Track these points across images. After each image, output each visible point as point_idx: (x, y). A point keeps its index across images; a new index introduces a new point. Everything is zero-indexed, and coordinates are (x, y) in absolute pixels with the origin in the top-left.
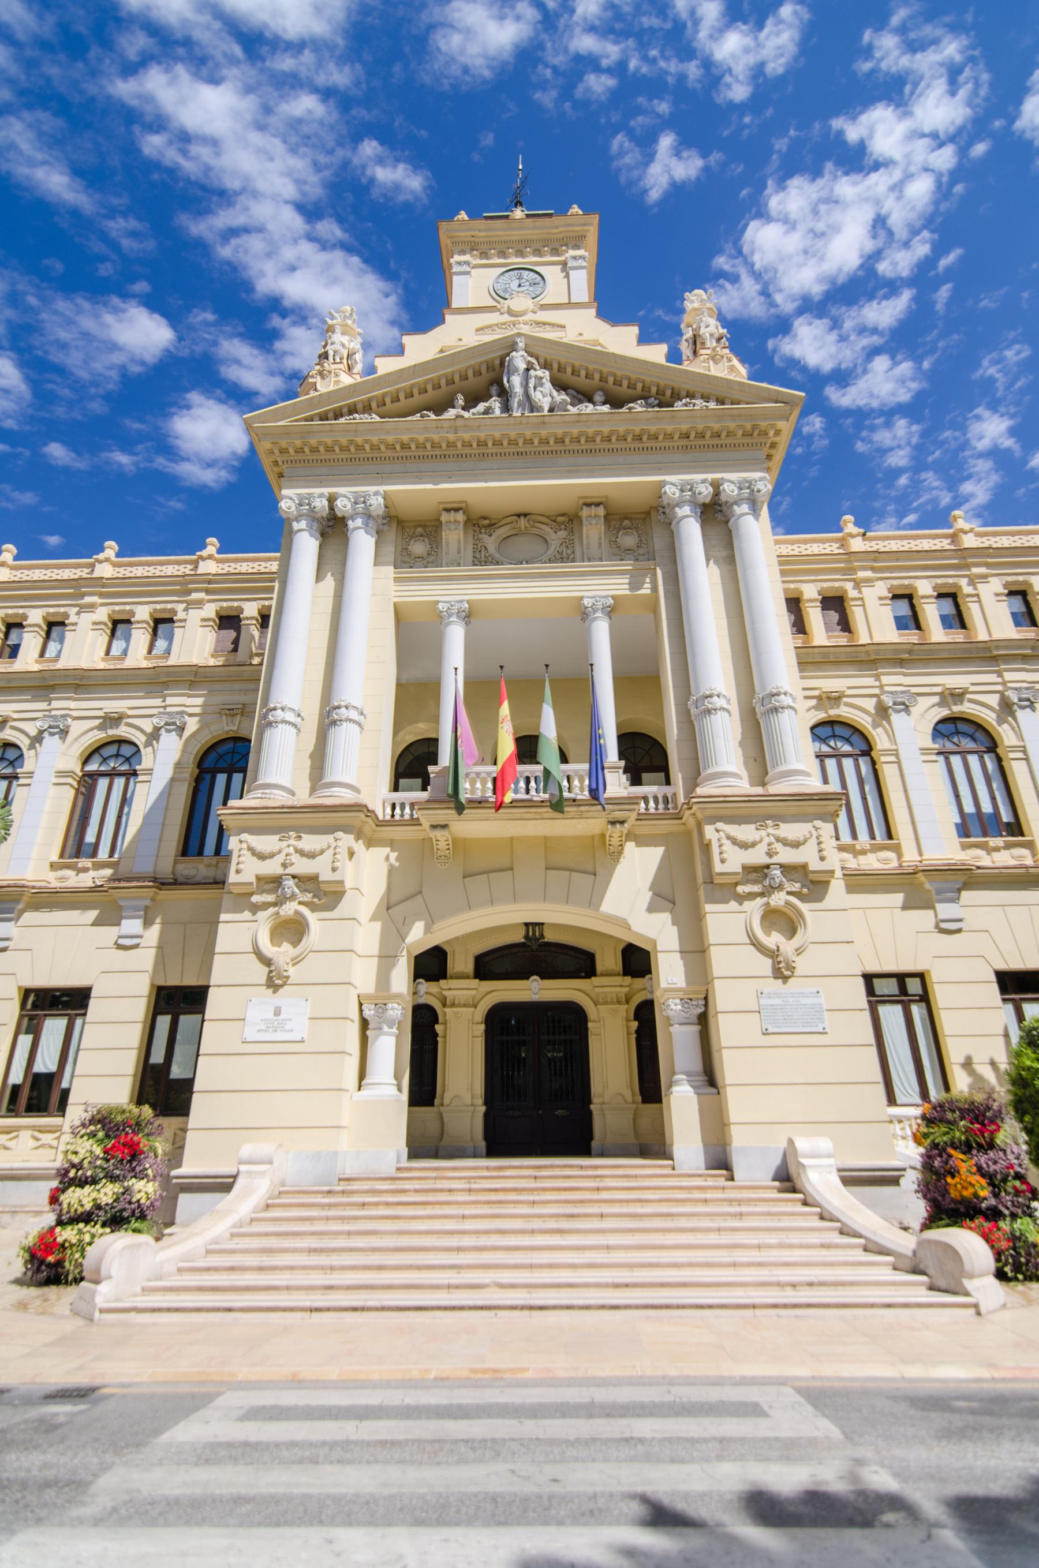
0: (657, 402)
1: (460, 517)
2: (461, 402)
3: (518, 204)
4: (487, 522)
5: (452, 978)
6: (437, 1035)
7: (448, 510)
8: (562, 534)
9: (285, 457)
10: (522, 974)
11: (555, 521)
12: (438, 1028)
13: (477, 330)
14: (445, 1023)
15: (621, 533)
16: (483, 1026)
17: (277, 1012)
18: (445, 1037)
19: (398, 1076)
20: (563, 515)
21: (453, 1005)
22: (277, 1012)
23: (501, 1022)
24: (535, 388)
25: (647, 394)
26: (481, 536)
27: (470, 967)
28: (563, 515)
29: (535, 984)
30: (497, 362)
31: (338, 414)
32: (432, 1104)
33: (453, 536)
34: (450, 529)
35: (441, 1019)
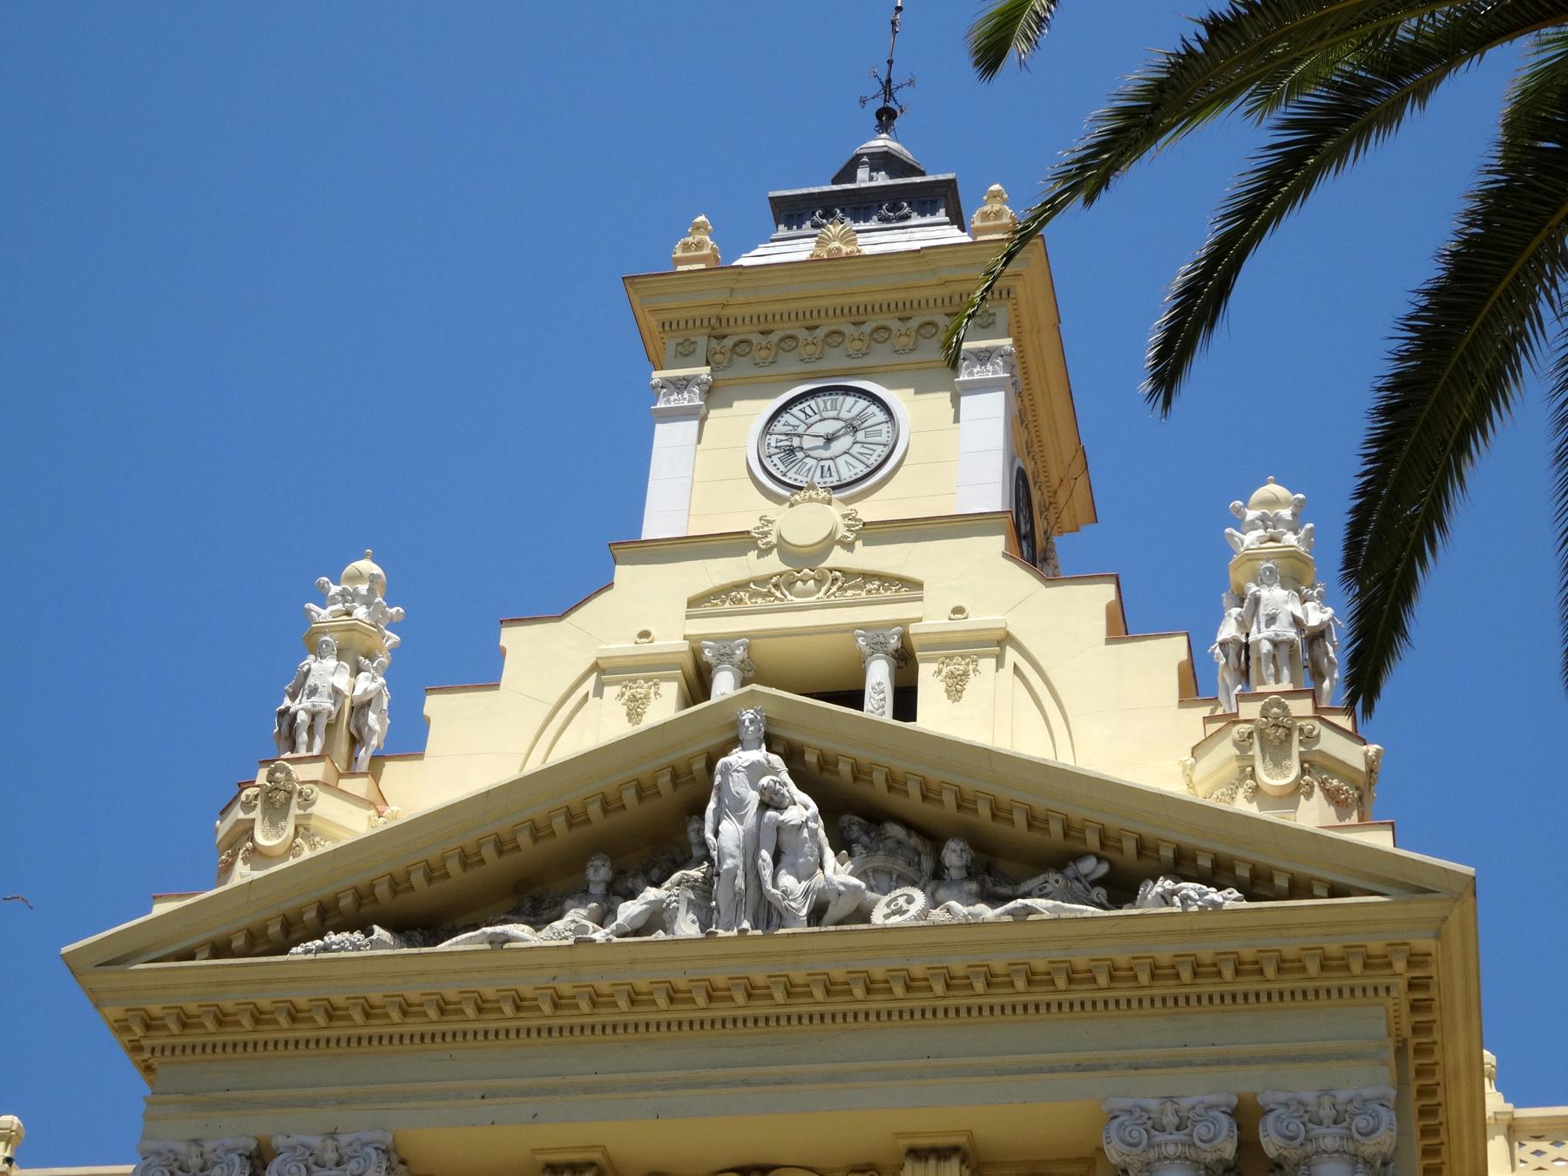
0: (1104, 869)
2: (598, 873)
3: (886, 118)
9: (158, 1039)
13: (693, 603)
24: (777, 858)
25: (1079, 847)
30: (700, 765)
31: (293, 931)
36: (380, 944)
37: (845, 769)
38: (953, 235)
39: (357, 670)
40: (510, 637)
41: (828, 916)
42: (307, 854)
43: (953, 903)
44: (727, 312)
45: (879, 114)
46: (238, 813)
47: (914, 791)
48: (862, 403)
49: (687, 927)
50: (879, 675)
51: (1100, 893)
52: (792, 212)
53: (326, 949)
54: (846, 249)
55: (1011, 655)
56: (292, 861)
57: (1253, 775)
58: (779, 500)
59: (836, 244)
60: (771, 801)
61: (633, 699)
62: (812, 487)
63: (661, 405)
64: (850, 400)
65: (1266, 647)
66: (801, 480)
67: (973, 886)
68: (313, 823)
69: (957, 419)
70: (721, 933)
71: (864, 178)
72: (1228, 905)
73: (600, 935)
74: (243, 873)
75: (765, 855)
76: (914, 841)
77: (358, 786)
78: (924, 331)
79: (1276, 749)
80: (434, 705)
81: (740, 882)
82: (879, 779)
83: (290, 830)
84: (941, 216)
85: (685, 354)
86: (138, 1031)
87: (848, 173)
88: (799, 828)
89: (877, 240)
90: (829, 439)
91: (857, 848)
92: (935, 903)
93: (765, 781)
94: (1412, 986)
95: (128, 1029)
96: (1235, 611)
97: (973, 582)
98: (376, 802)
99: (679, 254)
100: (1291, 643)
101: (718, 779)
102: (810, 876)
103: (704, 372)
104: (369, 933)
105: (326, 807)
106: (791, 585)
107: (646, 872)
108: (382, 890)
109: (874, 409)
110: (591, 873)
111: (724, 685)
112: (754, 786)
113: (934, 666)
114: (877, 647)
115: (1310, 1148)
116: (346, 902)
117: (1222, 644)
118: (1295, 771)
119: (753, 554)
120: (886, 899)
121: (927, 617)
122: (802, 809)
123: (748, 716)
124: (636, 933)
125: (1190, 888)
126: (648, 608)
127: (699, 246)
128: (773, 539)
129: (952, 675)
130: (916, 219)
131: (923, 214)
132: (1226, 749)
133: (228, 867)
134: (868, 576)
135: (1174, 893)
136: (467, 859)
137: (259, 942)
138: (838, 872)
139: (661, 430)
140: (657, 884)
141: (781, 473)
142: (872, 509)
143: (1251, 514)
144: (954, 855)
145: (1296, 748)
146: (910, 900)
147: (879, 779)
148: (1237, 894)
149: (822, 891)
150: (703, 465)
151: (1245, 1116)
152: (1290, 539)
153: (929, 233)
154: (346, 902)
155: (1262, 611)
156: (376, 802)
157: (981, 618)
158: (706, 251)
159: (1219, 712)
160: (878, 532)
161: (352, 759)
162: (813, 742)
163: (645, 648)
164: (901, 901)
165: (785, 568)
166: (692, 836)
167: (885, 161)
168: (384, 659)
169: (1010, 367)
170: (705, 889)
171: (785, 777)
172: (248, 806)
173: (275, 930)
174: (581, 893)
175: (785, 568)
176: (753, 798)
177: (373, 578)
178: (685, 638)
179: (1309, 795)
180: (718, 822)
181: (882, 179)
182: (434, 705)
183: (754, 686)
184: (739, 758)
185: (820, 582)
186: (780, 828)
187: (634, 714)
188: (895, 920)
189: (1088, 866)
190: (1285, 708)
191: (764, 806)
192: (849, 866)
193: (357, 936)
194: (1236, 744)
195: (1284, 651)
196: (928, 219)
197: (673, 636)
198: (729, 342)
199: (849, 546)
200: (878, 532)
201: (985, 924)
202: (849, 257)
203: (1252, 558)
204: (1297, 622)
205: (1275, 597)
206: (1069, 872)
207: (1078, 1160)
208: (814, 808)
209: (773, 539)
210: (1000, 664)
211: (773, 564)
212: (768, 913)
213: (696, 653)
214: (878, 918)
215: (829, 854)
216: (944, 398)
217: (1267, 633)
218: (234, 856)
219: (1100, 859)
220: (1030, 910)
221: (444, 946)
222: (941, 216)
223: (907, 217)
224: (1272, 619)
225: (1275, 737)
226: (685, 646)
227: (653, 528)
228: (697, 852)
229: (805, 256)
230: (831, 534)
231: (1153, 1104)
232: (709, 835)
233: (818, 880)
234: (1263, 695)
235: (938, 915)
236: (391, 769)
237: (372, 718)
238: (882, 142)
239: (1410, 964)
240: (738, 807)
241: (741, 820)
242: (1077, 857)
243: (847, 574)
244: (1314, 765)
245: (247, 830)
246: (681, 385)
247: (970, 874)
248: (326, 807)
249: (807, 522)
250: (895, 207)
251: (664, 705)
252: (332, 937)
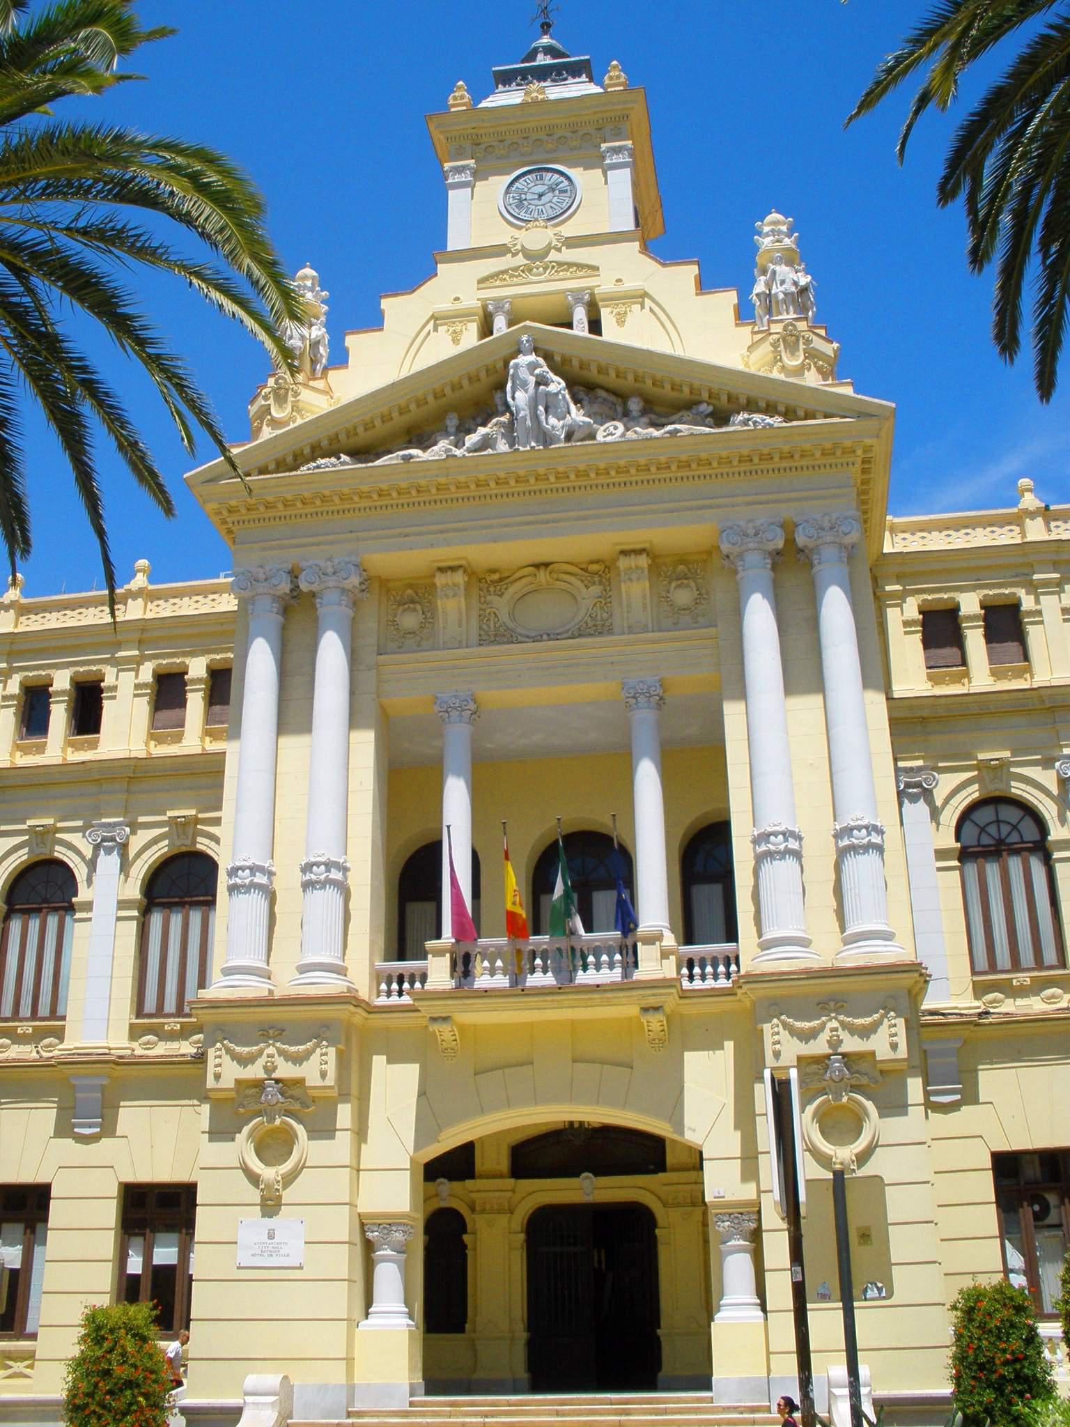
0: (711, 409)
1: (459, 578)
2: (452, 422)
3: (546, 28)
4: (496, 577)
5: (481, 1177)
6: (465, 1247)
7: (442, 570)
8: (595, 590)
9: (235, 518)
10: (569, 1170)
11: (585, 570)
12: (466, 1237)
13: (480, 282)
14: (474, 1233)
15: (674, 584)
16: (522, 1236)
17: (271, 1236)
18: (475, 1250)
19: (407, 1303)
20: (597, 562)
21: (483, 1211)
22: (271, 1236)
23: (545, 1228)
26: (489, 598)
27: (504, 1164)
28: (597, 562)
29: (586, 1183)
30: (500, 365)
31: (298, 460)
32: (462, 1330)
33: (452, 607)
34: (447, 596)
35: (469, 1226)
36: (343, 463)
37: (576, 363)
38: (593, 89)
39: (311, 325)
40: (385, 304)
41: (574, 437)
42: (299, 421)
43: (637, 429)
44: (481, 131)
45: (542, 26)
46: (261, 402)
47: (613, 374)
48: (556, 176)
49: (502, 446)
52: (506, 79)
53: (318, 467)
54: (540, 97)
55: (647, 302)
56: (292, 426)
57: (781, 360)
58: (520, 228)
59: (534, 95)
60: (541, 381)
61: (455, 332)
62: (536, 220)
63: (450, 181)
64: (550, 174)
65: (781, 296)
66: (527, 217)
67: (645, 420)
68: (301, 405)
69: (606, 183)
70: (521, 449)
71: (543, 60)
73: (458, 452)
74: (267, 433)
75: (541, 408)
76: (612, 398)
77: (319, 384)
78: (578, 137)
79: (792, 348)
80: (351, 341)
81: (529, 423)
82: (594, 369)
83: (289, 409)
84: (584, 78)
85: (460, 155)
86: (225, 513)
87: (532, 56)
88: (557, 394)
89: (556, 92)
90: (540, 196)
91: (585, 403)
92: (627, 429)
93: (538, 371)
94: (863, 462)
95: (220, 513)
96: (763, 278)
97: (625, 267)
98: (328, 392)
99: (451, 102)
100: (792, 293)
101: (511, 371)
102: (564, 418)
103: (472, 162)
104: (339, 458)
105: (306, 395)
106: (530, 270)
107: (474, 419)
108: (343, 437)
109: (562, 179)
110: (448, 422)
111: (500, 323)
112: (532, 374)
113: (609, 309)
114: (578, 300)
115: (819, 541)
116: (325, 443)
117: (757, 295)
118: (802, 357)
119: (509, 255)
120: (602, 428)
121: (604, 284)
122: (557, 385)
123: (524, 338)
124: (475, 451)
125: (757, 417)
126: (455, 286)
127: (462, 97)
128: (519, 247)
129: (619, 314)
130: (571, 80)
131: (574, 77)
132: (766, 348)
133: (259, 429)
134: (570, 265)
135: (749, 420)
136: (385, 419)
137: (281, 466)
138: (577, 415)
139: (450, 193)
140: (484, 424)
141: (518, 211)
142: (571, 229)
143: (766, 229)
144: (635, 405)
145: (802, 347)
146: (616, 428)
147: (594, 369)
149: (570, 426)
150: (476, 210)
151: (789, 528)
152: (787, 241)
153: (578, 88)
154: (325, 443)
155: (778, 278)
156: (328, 392)
157: (630, 285)
158: (466, 100)
159: (756, 329)
160: (572, 242)
161: (314, 370)
162: (558, 350)
163: (458, 306)
165: (526, 262)
167: (549, 50)
168: (323, 319)
169: (631, 156)
170: (510, 427)
171: (546, 369)
172: (266, 398)
173: (290, 459)
174: (446, 434)
175: (526, 262)
176: (532, 380)
177: (313, 278)
179: (809, 369)
180: (514, 393)
181: (548, 60)
182: (351, 341)
183: (528, 323)
184: (523, 360)
185: (545, 269)
186: (547, 394)
187: (456, 341)
188: (609, 439)
189: (704, 408)
190: (794, 326)
191: (538, 384)
192: (582, 412)
193: (333, 460)
194: (772, 345)
195: (789, 299)
196: (577, 80)
197: (472, 299)
198: (483, 146)
199: (559, 250)
200: (572, 242)
201: (656, 438)
202: (543, 101)
203: (769, 251)
204: (795, 283)
205: (783, 270)
206: (694, 411)
207: (702, 552)
208: (563, 384)
209: (519, 247)
210: (643, 307)
211: (520, 260)
212: (546, 438)
213: (485, 307)
214: (600, 437)
215: (573, 407)
216: (600, 171)
217: (781, 289)
218: (262, 423)
219: (708, 404)
220: (677, 431)
221: (378, 462)
222: (584, 78)
223: (566, 79)
224: (783, 282)
225: (790, 340)
226: (479, 304)
227: (451, 247)
228: (501, 408)
229: (519, 101)
230: (550, 244)
231: (742, 523)
232: (509, 399)
233: (568, 420)
234: (781, 321)
235: (630, 435)
236: (332, 374)
237: (321, 349)
238: (545, 40)
239: (865, 452)
240: (524, 385)
241: (526, 391)
242: (699, 403)
243: (560, 264)
244: (811, 354)
245: (267, 410)
246: (459, 170)
247: (644, 412)
248: (306, 395)
249: (536, 237)
250: (559, 74)
251: (470, 337)
252: (321, 461)
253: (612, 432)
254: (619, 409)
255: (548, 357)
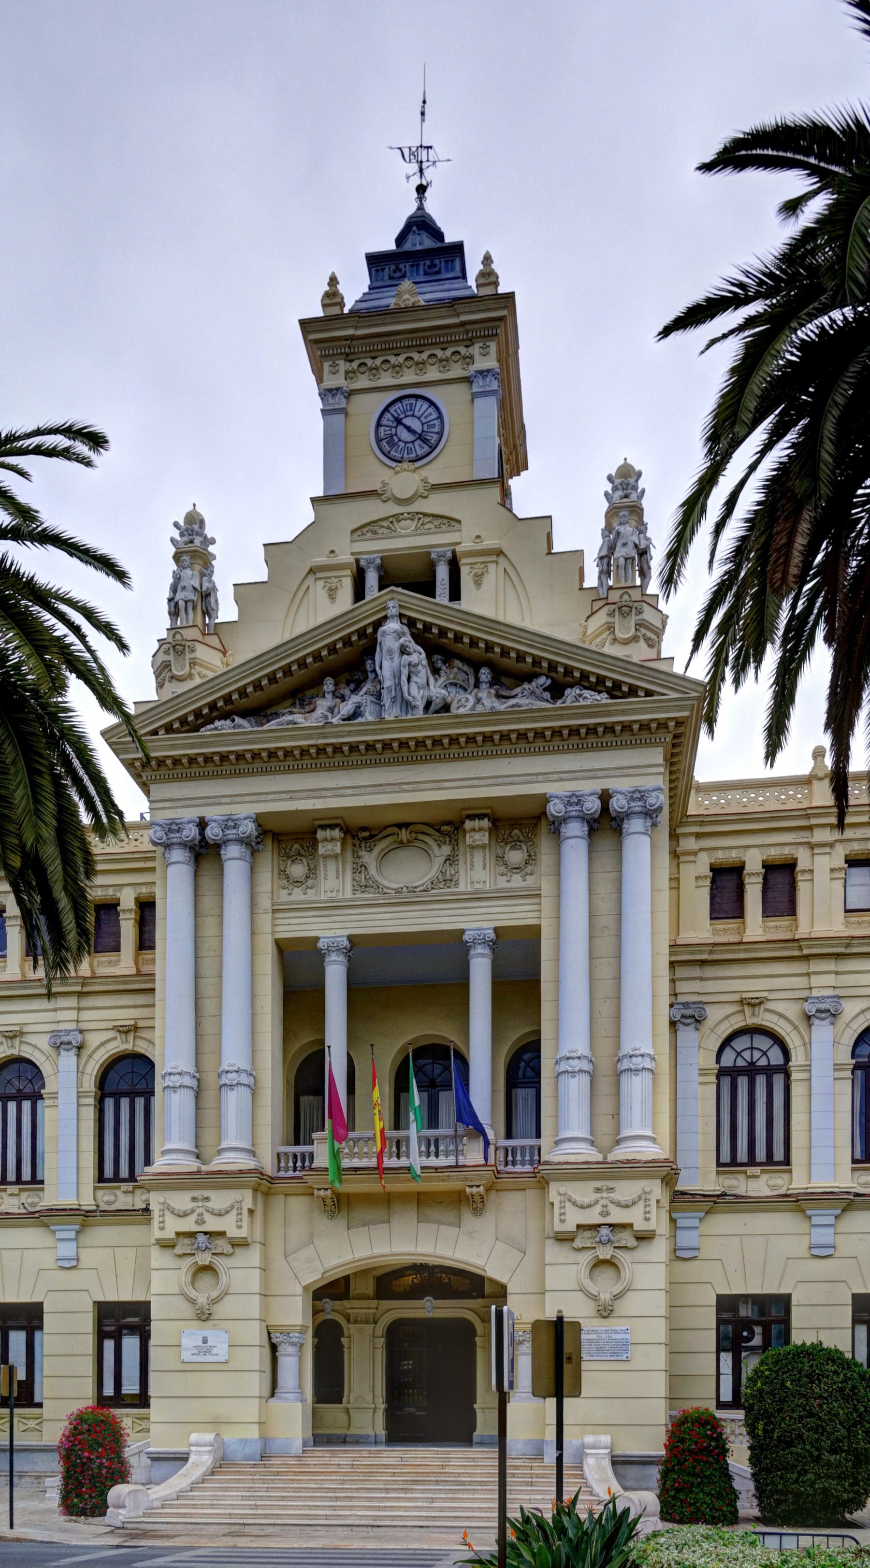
41: (432, 708)
50: (442, 573)
51: (547, 695)
72: (604, 701)
104: (233, 721)
122: (418, 655)
125: (587, 693)
129: (476, 575)
135: (580, 696)
148: (606, 696)
164: (463, 700)
166: (369, 667)
178: (352, 554)
212: (408, 706)
213: (357, 561)
219: (547, 677)
226: (352, 559)
242: (537, 675)
252: (218, 723)
253: (465, 703)
254: (472, 680)
255: (411, 623)
